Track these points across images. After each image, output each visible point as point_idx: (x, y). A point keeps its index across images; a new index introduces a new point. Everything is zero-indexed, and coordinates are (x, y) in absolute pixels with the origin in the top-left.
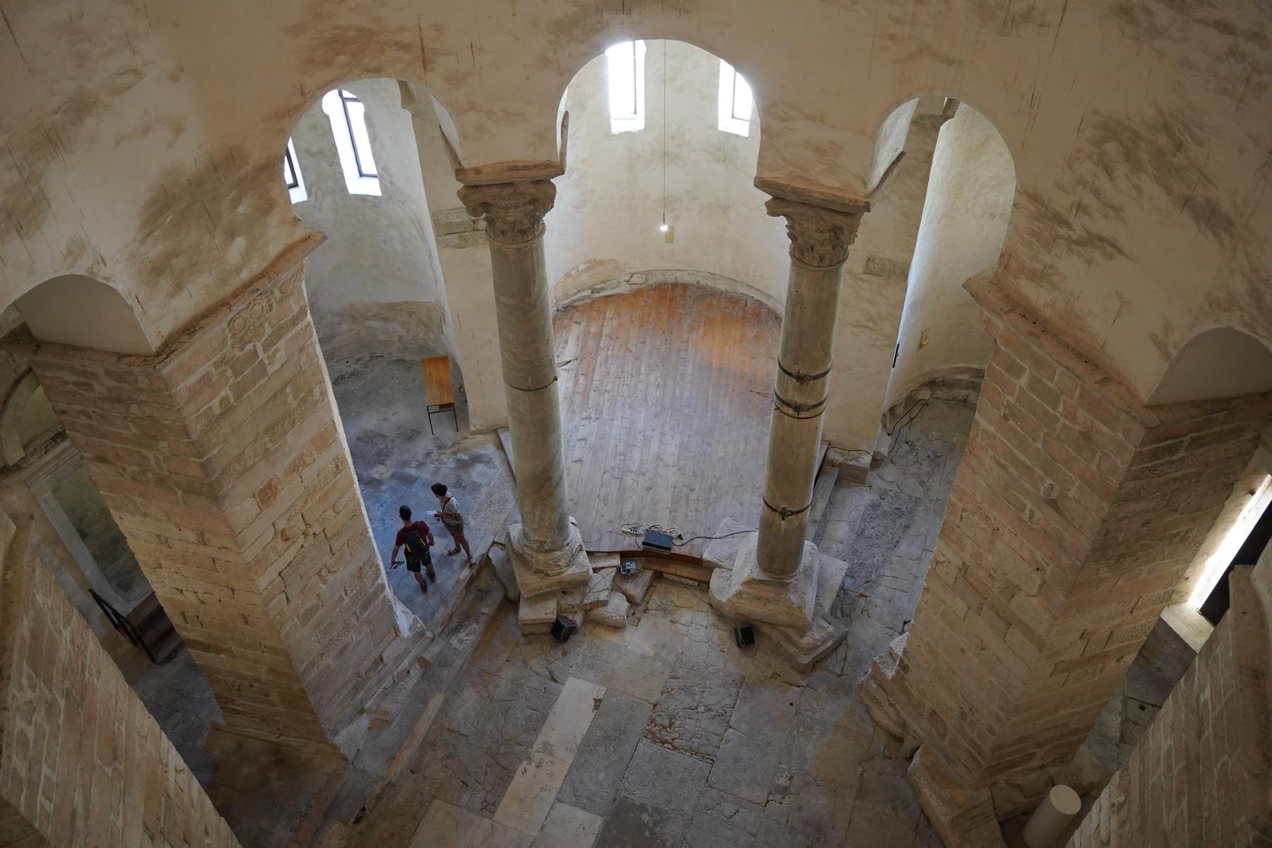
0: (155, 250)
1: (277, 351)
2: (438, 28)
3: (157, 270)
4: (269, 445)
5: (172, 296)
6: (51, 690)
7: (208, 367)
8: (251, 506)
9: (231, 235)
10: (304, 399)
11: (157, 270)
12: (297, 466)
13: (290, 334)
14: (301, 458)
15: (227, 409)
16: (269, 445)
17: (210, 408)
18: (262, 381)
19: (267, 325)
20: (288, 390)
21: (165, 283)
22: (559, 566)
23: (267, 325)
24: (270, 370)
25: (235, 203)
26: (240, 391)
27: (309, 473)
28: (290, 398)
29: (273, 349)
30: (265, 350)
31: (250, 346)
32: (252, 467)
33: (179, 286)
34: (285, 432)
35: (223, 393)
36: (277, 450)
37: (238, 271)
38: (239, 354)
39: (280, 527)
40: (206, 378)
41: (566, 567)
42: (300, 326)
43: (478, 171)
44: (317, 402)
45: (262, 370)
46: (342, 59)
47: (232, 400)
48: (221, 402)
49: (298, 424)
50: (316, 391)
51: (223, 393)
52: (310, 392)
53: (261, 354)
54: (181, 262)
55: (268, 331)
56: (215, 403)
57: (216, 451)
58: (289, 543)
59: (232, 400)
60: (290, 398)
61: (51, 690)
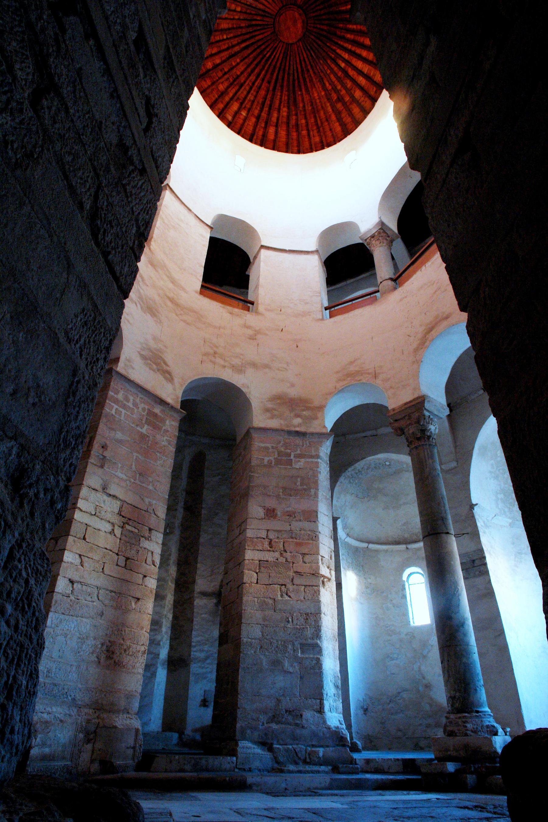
0: (270, 405)
1: (299, 461)
2: (381, 367)
3: (267, 410)
4: (281, 494)
5: (268, 418)
6: (146, 423)
7: (269, 445)
8: (261, 513)
9: (298, 416)
10: (305, 490)
11: (267, 410)
12: (291, 515)
13: (308, 460)
14: (294, 513)
15: (269, 465)
16: (281, 494)
17: (264, 459)
18: (289, 467)
19: (299, 450)
20: (299, 479)
21: (268, 414)
22: (466, 727)
23: (299, 450)
24: (294, 466)
25: (304, 410)
26: (278, 462)
27: (296, 525)
28: (298, 483)
29: (298, 459)
30: (294, 457)
31: (289, 451)
32: (270, 496)
33: (272, 417)
34: (291, 496)
35: (271, 458)
36: (283, 499)
37: (295, 427)
38: (282, 449)
39: (272, 536)
40: (267, 448)
41: (472, 731)
42: (313, 460)
43: (394, 410)
44: (311, 496)
45: (290, 462)
46: (349, 379)
47: (273, 463)
48: (268, 461)
49: (299, 497)
50: (313, 491)
51: (271, 458)
52: (310, 489)
53: (292, 457)
54: (276, 413)
55: (298, 452)
56: (266, 459)
57: (257, 475)
58: (271, 549)
59: (273, 463)
60: (298, 483)
61: (146, 423)
